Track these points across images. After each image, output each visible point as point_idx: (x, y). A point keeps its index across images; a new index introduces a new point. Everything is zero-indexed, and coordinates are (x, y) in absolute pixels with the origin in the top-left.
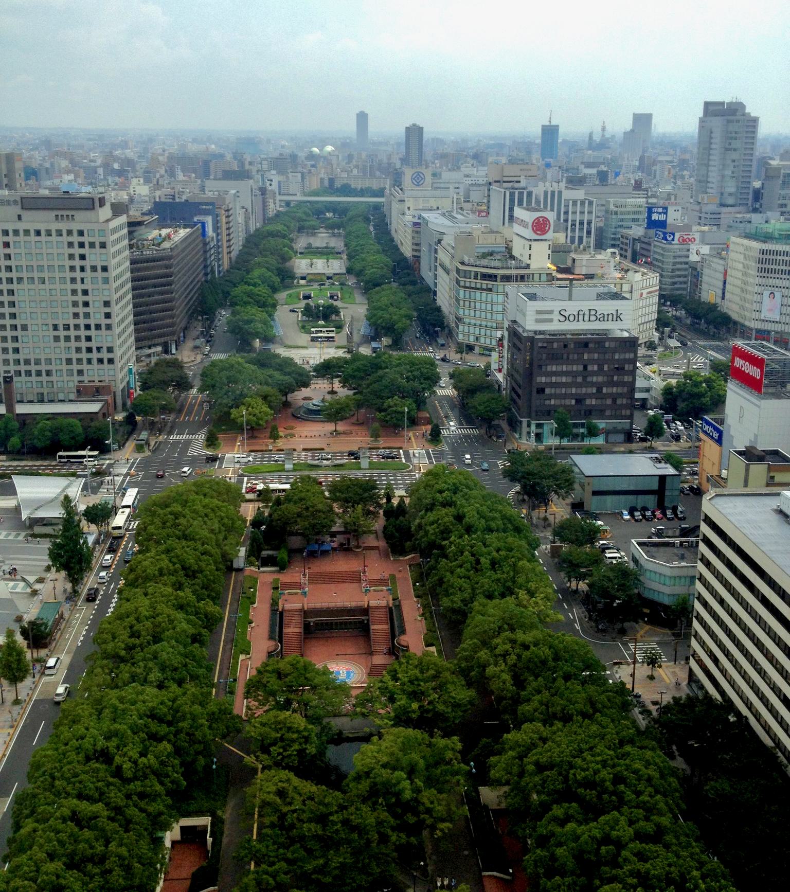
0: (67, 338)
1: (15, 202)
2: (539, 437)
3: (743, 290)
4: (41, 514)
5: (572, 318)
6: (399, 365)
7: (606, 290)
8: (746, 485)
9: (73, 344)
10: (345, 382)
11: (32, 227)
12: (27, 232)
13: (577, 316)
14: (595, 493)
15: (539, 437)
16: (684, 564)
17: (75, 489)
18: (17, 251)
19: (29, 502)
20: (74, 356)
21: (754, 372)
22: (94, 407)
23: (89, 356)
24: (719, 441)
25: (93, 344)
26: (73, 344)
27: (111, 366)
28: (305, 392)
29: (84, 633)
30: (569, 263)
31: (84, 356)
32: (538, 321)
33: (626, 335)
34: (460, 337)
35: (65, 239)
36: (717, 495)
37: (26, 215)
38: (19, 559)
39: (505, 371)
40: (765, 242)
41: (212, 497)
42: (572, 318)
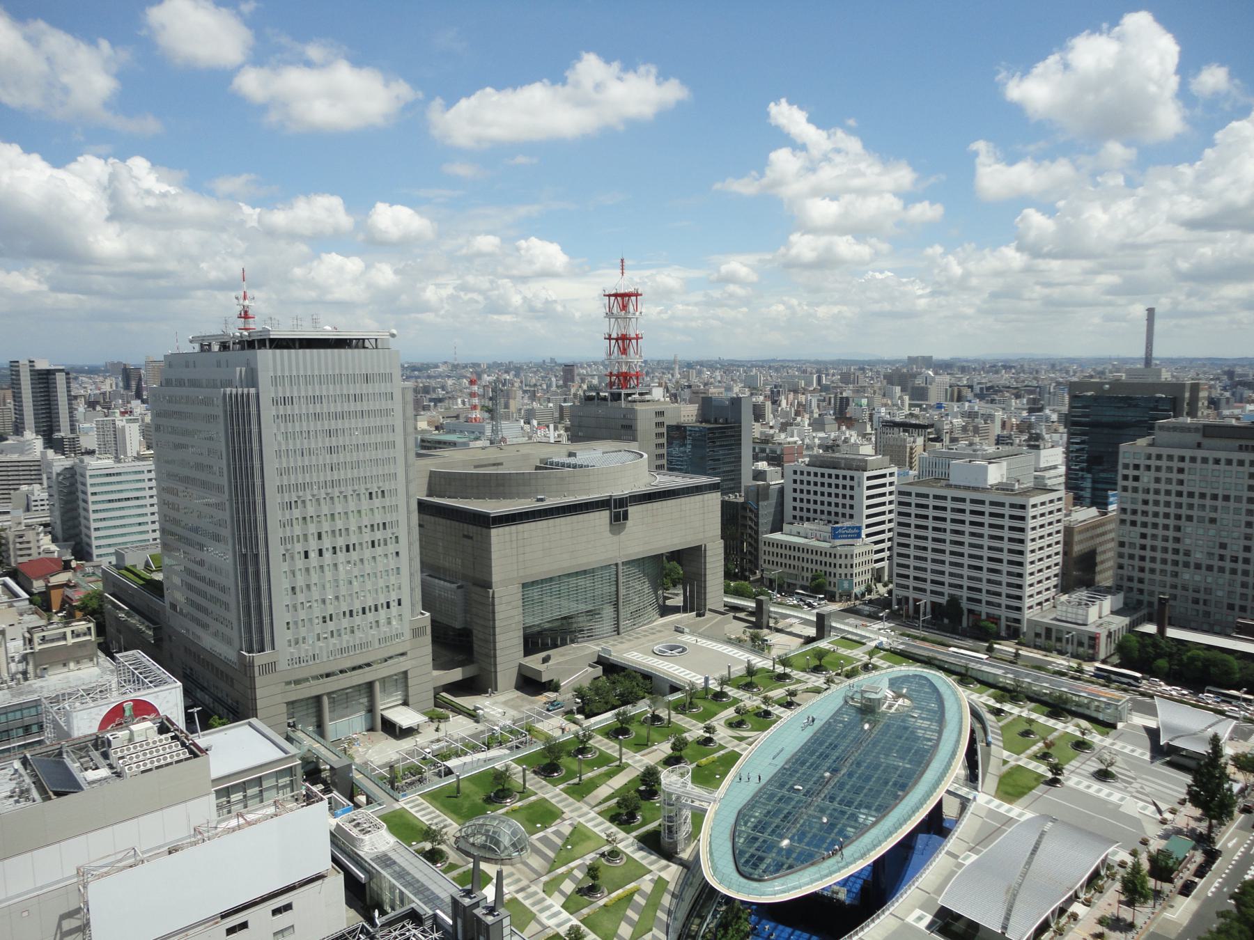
0: (1234, 572)
1: (1196, 430)
4: (1176, 743)
12: (1205, 460)
17: (1225, 729)
18: (1191, 477)
19: (1170, 729)
20: (1239, 590)
29: (1217, 885)
37: (1206, 442)
38: (1154, 782)
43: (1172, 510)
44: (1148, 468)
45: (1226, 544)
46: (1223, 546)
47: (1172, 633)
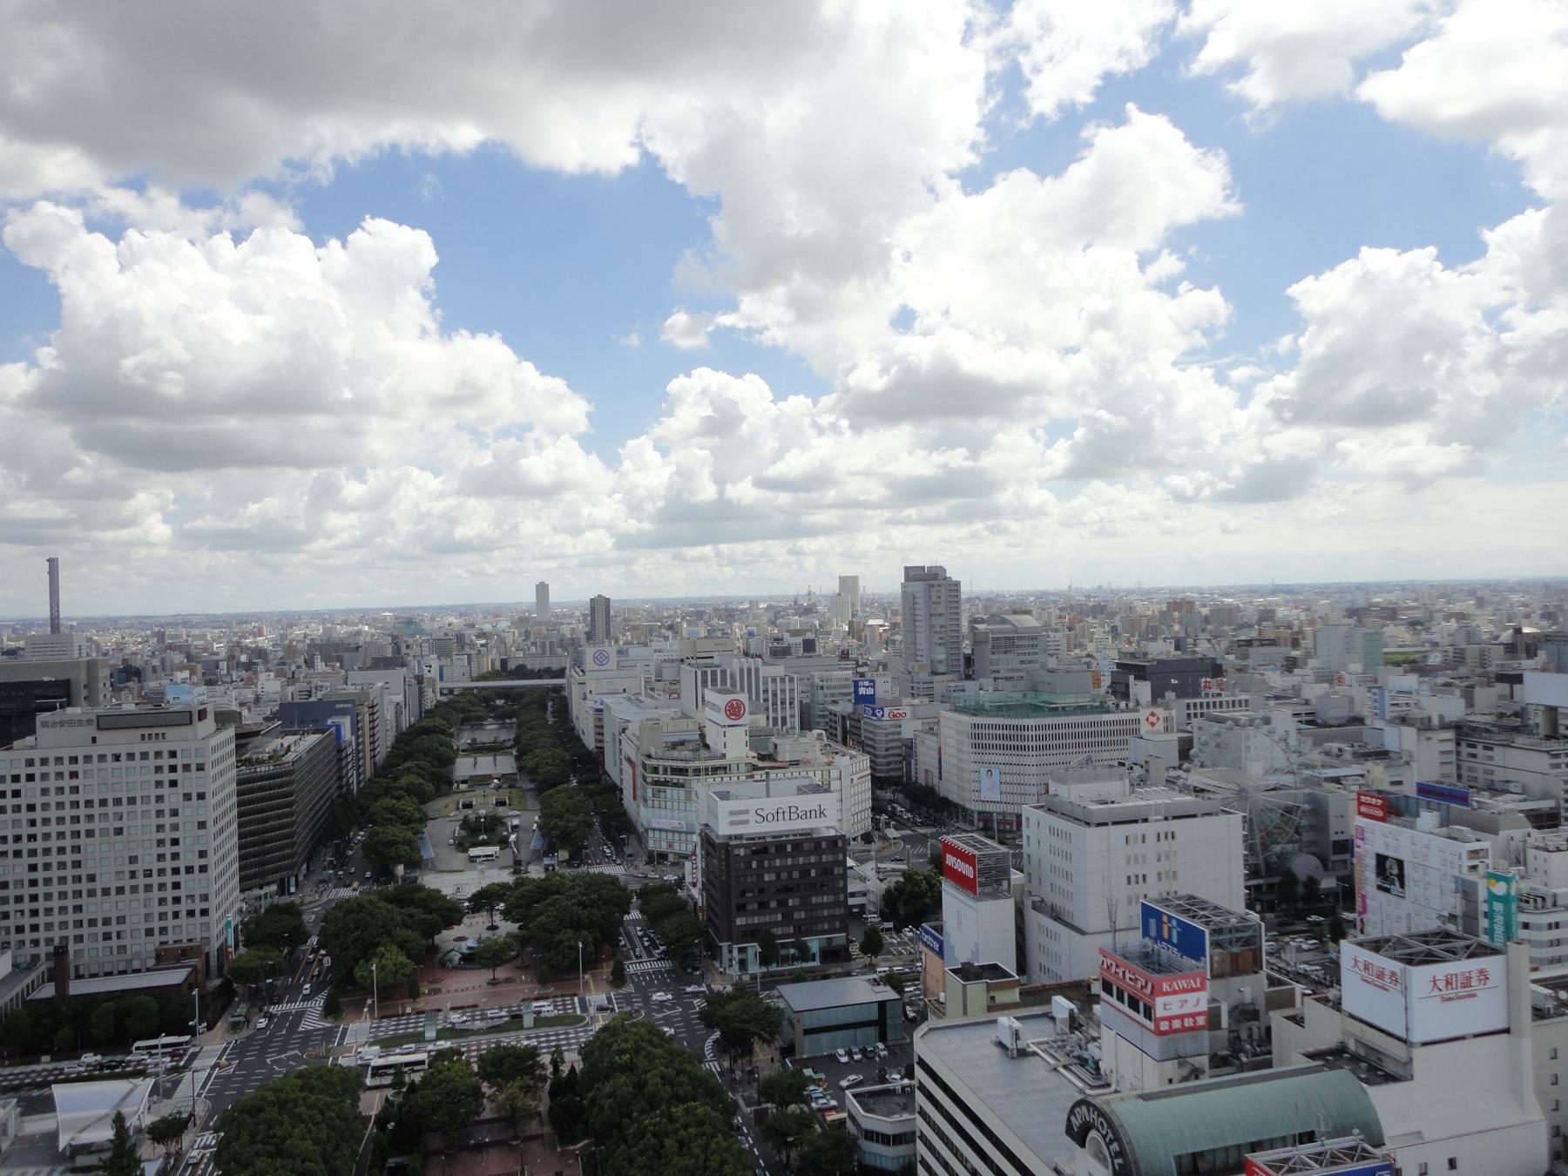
0: (148, 888)
1: (89, 722)
2: (743, 964)
3: (959, 769)
5: (770, 818)
6: (573, 888)
7: (806, 782)
8: (965, 1013)
9: (156, 894)
10: (506, 915)
11: (109, 752)
12: (102, 758)
13: (776, 815)
14: (807, 1032)
15: (743, 964)
16: (906, 1116)
18: (87, 782)
21: (967, 870)
22: (175, 977)
23: (176, 908)
24: (940, 953)
25: (182, 893)
26: (156, 894)
27: (205, 919)
28: (457, 931)
30: (771, 749)
31: (169, 908)
32: (732, 823)
33: (832, 833)
34: (651, 845)
35: (152, 762)
36: (930, 1030)
37: (102, 736)
39: (699, 885)
40: (976, 715)
41: (321, 1092)
42: (770, 818)
43: (68, 828)
44: (30, 778)
45: (136, 857)
46: (133, 860)
47: (76, 988)
